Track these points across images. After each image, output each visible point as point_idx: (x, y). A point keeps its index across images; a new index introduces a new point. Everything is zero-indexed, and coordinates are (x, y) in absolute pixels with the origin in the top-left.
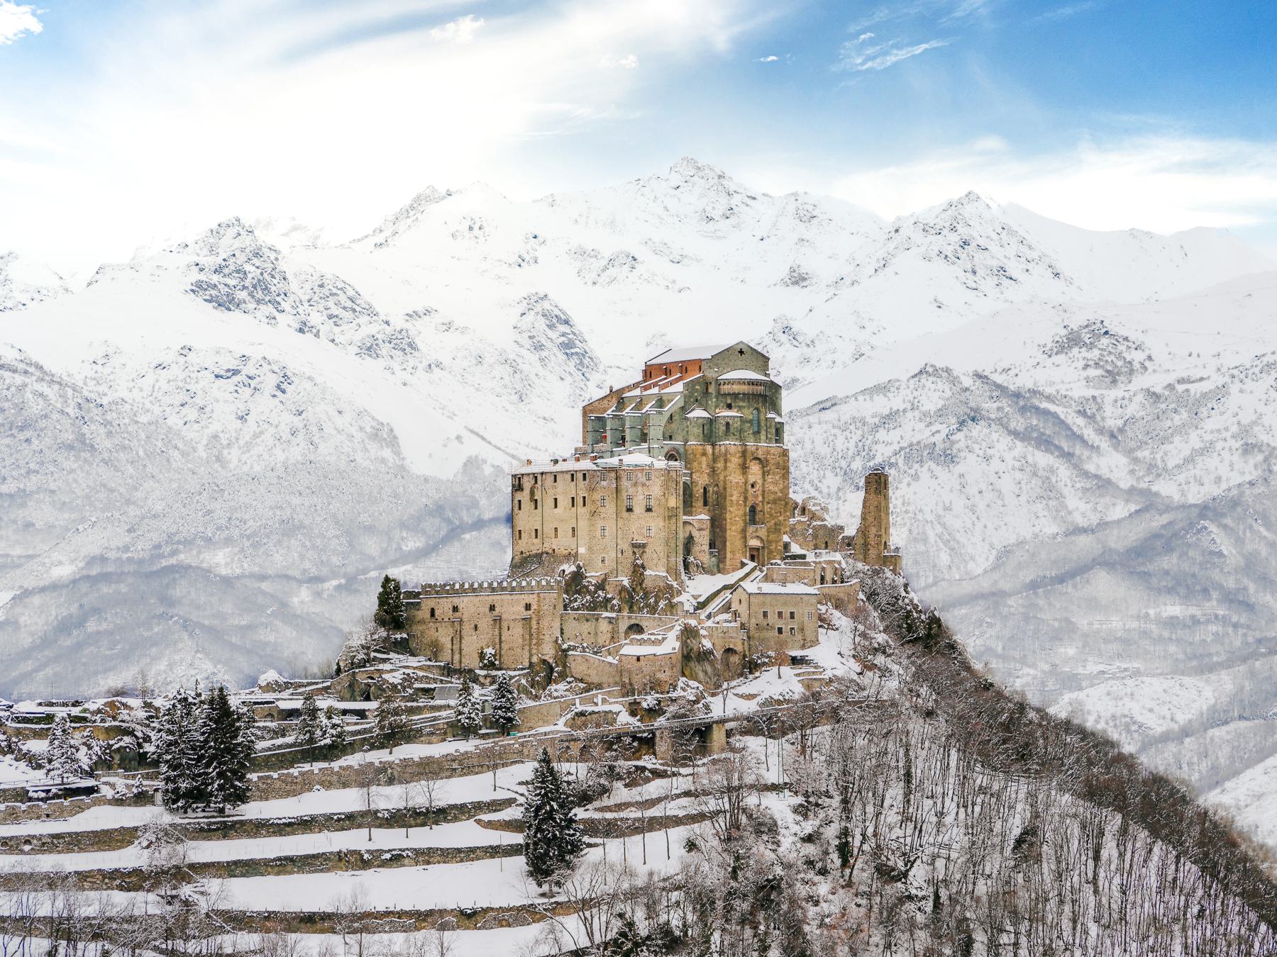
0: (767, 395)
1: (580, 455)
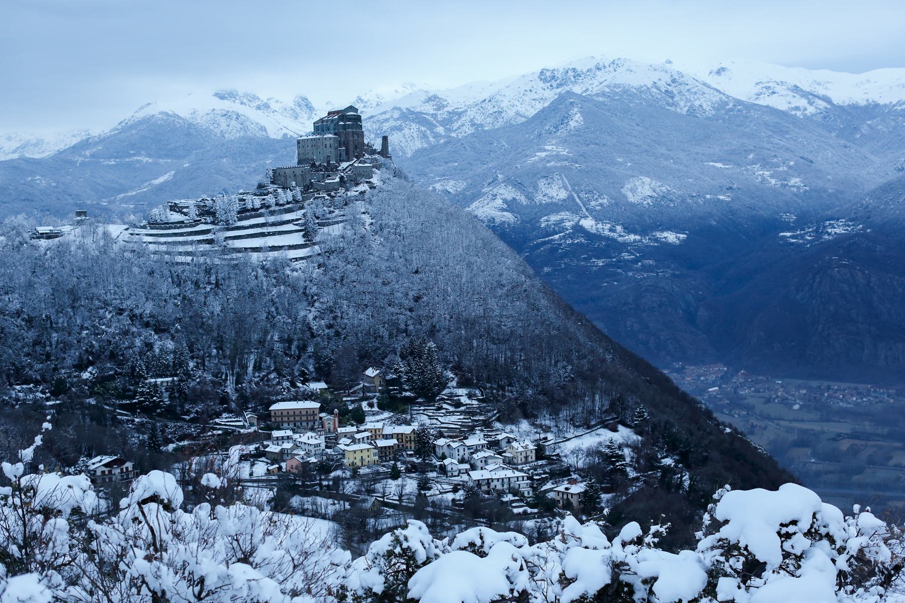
0: (358, 118)
1: (313, 134)
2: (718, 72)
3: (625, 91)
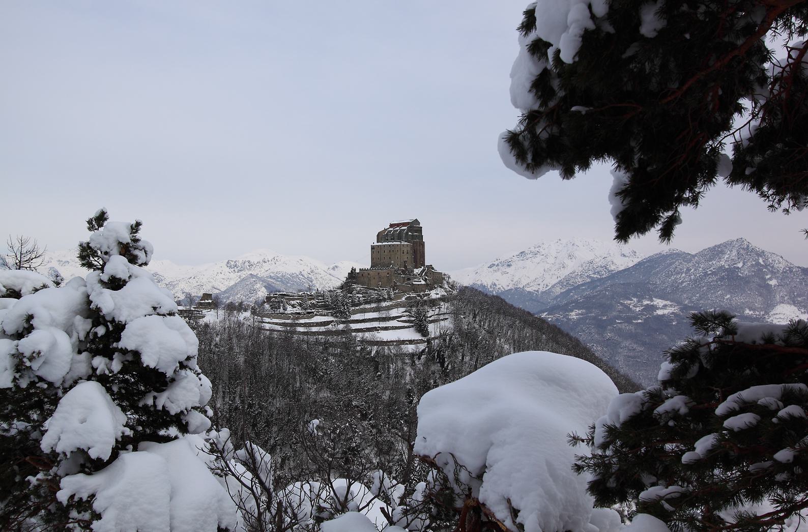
2: (333, 269)
3: (283, 276)
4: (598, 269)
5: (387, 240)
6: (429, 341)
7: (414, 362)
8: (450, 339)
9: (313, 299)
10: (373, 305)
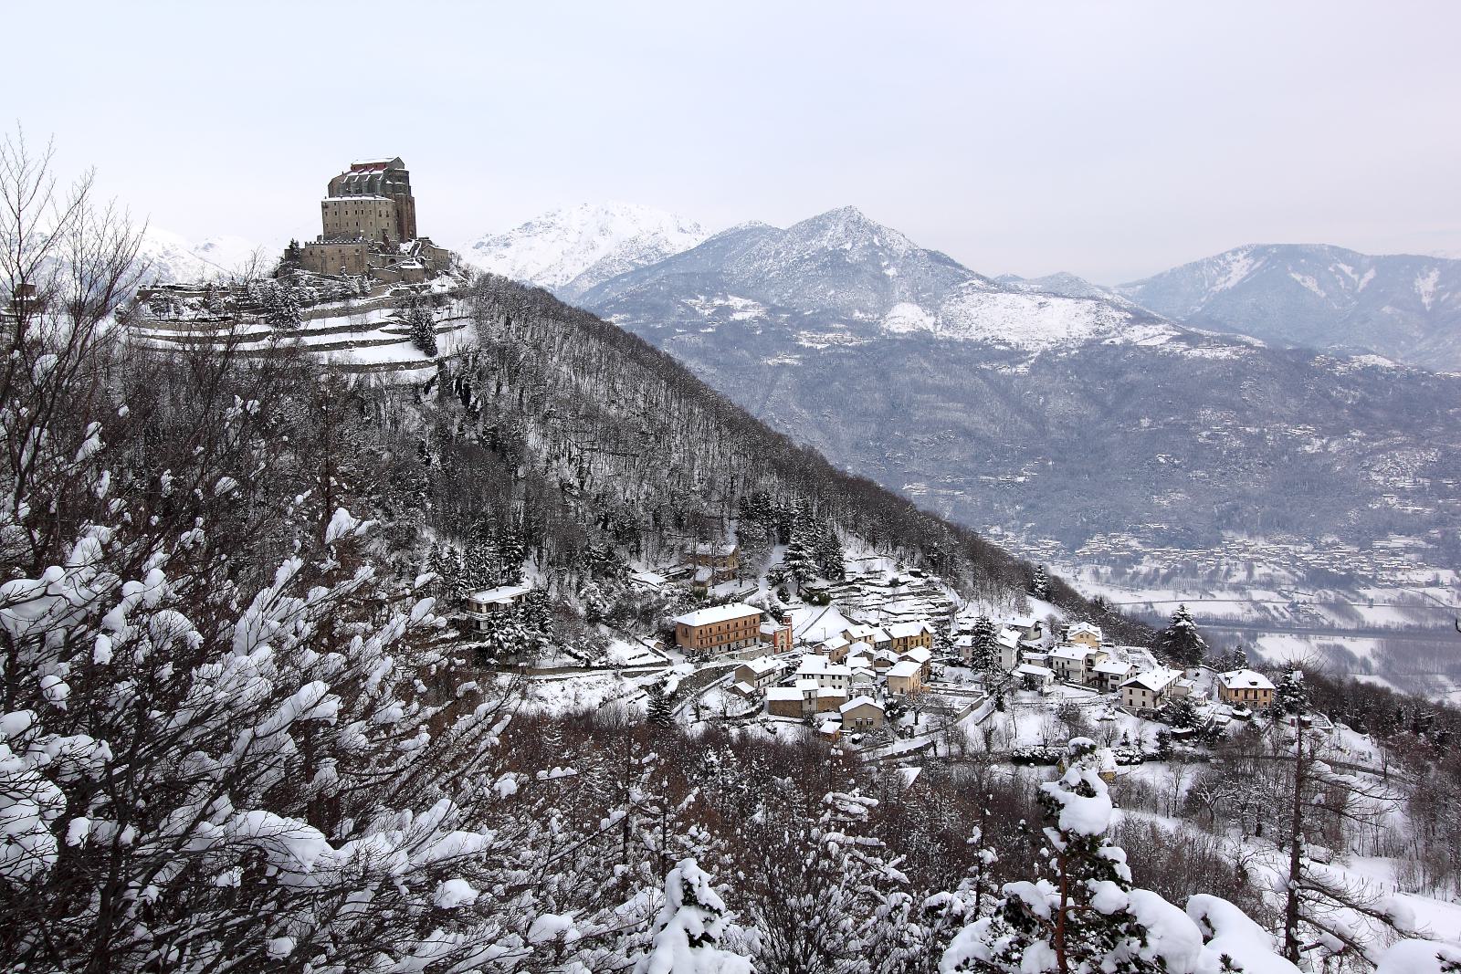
4: (645, 252)
5: (348, 193)
6: (441, 363)
7: (419, 397)
8: (475, 359)
9: (228, 294)
10: (337, 305)
